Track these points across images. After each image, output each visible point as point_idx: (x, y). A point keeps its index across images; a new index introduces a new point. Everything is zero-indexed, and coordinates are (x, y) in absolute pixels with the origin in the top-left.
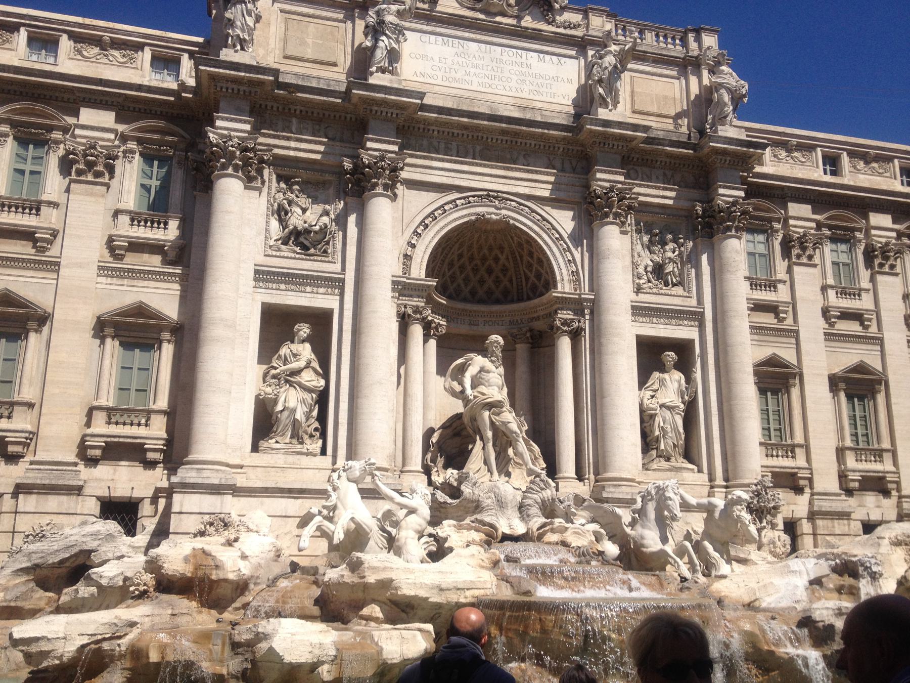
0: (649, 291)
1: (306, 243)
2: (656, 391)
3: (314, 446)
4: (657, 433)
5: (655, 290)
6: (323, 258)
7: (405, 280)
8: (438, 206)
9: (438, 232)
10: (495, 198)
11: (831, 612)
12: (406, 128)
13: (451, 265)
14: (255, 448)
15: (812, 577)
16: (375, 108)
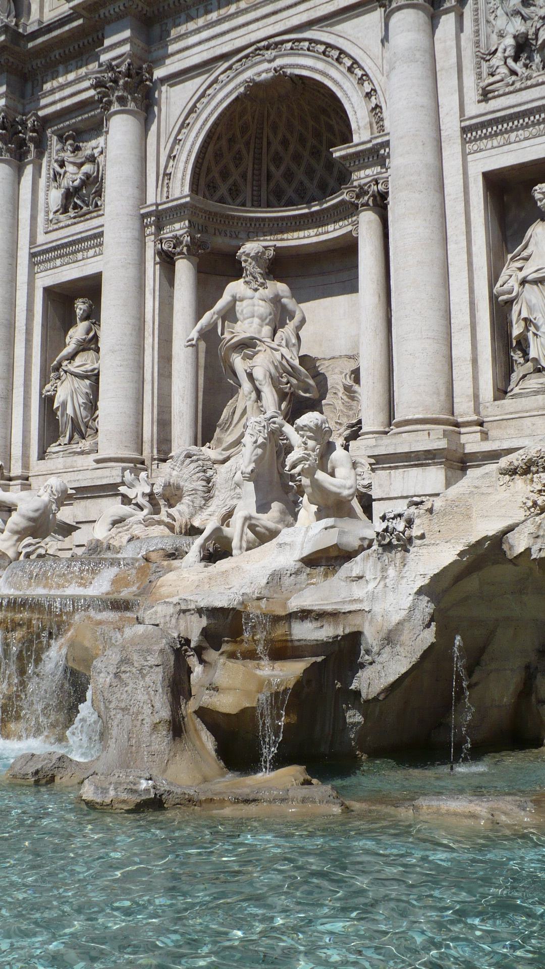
0: (501, 92)
1: (78, 202)
2: (526, 259)
3: (88, 443)
4: (516, 331)
5: (518, 85)
6: (94, 214)
7: (154, 208)
8: (199, 93)
9: (201, 128)
10: (267, 48)
11: (171, 610)
12: (156, 12)
13: (277, 160)
14: (42, 455)
15: (305, 553)
16: (102, 12)
